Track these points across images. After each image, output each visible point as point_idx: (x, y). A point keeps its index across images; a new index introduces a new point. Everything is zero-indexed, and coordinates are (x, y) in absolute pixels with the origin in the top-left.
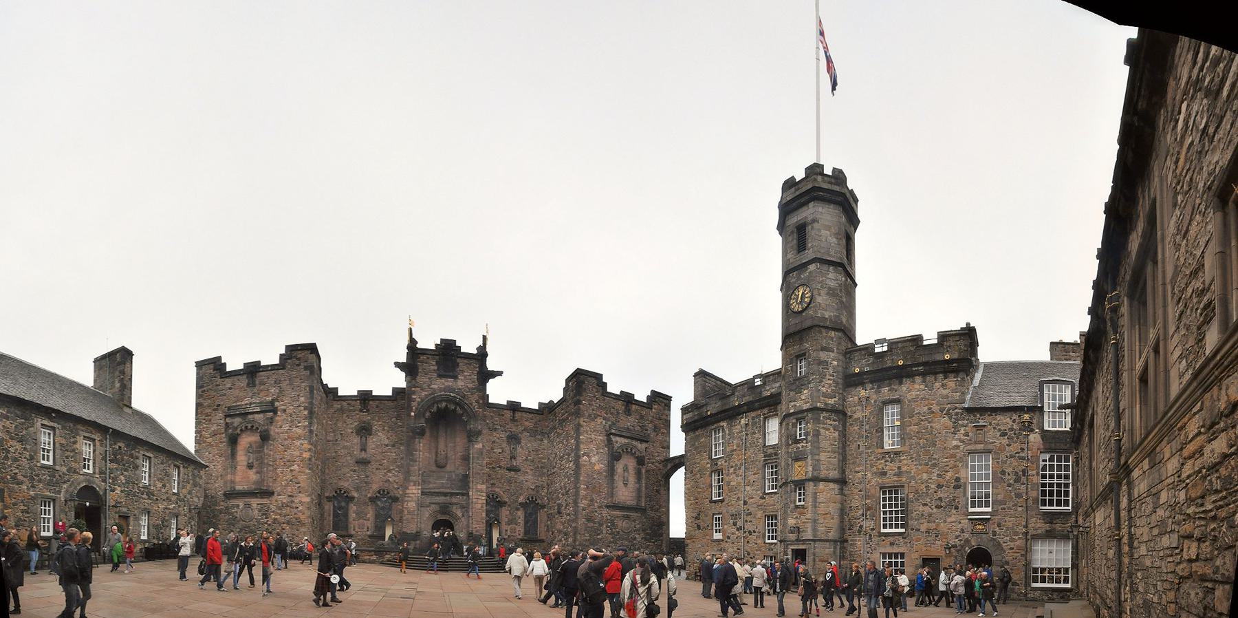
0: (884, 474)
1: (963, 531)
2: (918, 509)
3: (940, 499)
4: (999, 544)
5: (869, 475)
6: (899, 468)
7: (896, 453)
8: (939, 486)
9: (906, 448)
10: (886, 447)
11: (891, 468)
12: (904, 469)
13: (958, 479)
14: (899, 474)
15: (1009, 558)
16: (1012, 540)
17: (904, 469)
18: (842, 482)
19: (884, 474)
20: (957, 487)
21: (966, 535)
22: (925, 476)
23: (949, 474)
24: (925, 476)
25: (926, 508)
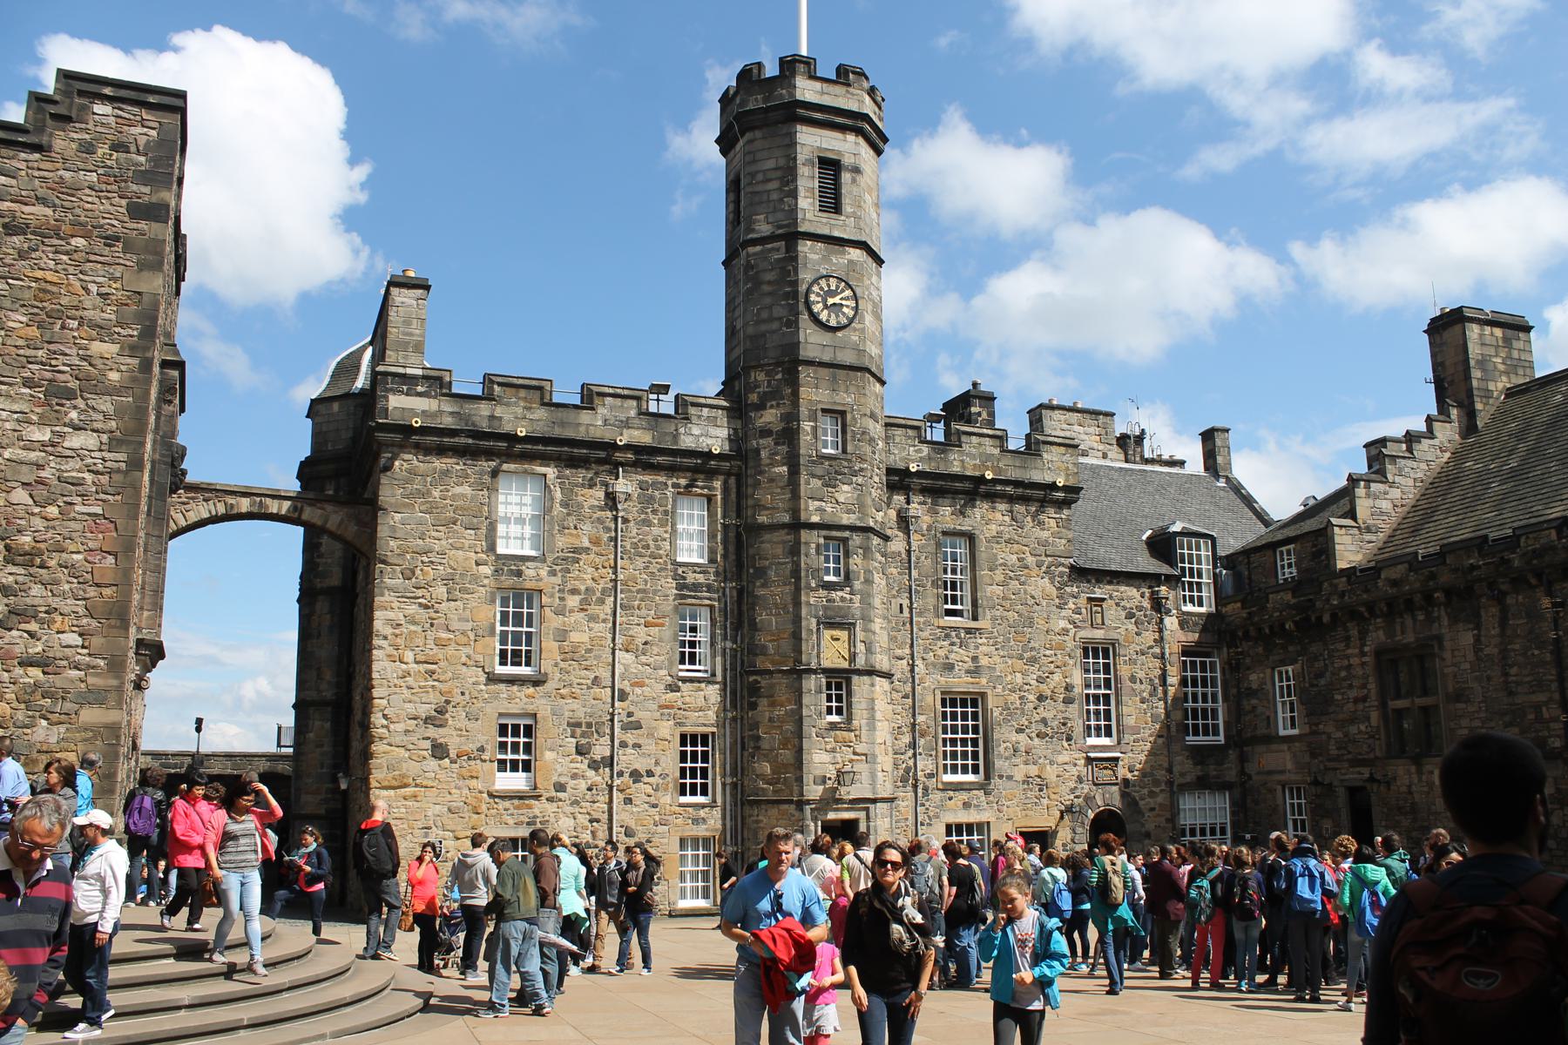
0: (949, 667)
1: (1080, 780)
2: (1005, 737)
3: (1044, 721)
4: (1136, 803)
6: (975, 659)
7: (969, 631)
8: (1041, 698)
11: (960, 655)
13: (1069, 688)
14: (975, 671)
15: (1150, 826)
16: (1152, 794)
17: (984, 661)
18: (888, 676)
19: (949, 667)
20: (1068, 701)
21: (1086, 788)
23: (1057, 677)
24: (1019, 678)
25: (1022, 737)
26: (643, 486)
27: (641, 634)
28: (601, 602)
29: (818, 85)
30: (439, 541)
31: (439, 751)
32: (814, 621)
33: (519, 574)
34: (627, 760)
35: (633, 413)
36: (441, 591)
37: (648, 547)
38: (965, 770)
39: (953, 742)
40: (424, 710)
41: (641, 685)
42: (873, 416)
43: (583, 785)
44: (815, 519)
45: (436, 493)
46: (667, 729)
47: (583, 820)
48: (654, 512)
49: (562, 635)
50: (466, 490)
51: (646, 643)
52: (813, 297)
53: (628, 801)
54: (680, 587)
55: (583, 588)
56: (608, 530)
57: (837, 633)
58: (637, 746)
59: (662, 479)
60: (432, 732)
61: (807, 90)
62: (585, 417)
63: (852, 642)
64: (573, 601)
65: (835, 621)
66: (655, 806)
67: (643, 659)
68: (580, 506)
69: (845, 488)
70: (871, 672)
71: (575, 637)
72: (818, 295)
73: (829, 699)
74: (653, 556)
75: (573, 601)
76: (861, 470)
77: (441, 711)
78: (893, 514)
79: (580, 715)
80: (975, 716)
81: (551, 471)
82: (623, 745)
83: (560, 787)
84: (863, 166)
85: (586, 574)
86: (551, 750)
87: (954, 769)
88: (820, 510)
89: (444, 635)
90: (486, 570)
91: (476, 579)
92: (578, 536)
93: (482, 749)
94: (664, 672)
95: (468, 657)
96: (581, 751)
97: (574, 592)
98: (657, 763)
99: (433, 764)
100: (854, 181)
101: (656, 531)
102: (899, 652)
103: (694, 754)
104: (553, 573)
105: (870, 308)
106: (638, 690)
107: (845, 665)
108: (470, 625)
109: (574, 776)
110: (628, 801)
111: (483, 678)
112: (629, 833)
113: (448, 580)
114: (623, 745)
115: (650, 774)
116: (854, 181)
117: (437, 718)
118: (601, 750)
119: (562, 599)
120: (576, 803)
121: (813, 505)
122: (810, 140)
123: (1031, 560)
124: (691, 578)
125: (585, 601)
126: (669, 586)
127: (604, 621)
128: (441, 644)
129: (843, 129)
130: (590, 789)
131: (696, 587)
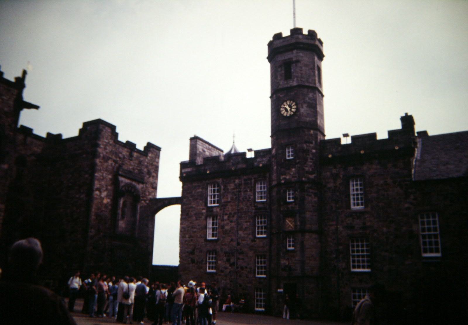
5: (340, 228)
9: (369, 209)
10: (352, 207)
12: (368, 224)
22: (385, 229)
24: (385, 229)
26: (245, 180)
27: (245, 225)
28: (233, 216)
29: (282, 41)
30: (194, 205)
31: (193, 261)
32: (281, 215)
33: (212, 211)
34: (240, 263)
35: (240, 160)
36: (194, 218)
37: (246, 198)
38: (364, 267)
39: (358, 256)
40: (190, 250)
41: (244, 240)
42: (306, 142)
43: (228, 271)
44: (283, 182)
45: (193, 192)
46: (251, 254)
47: (228, 281)
48: (249, 187)
49: (223, 227)
50: (200, 190)
51: (246, 228)
52: (282, 109)
53: (240, 276)
54: (256, 209)
55: (228, 213)
56: (235, 195)
57: (290, 219)
58: (243, 259)
59: (250, 176)
60: (191, 256)
61: (278, 43)
62: (227, 164)
63: (295, 221)
64: (226, 217)
65: (290, 214)
66: (247, 277)
67: (245, 232)
68: (228, 189)
69: (293, 169)
70: (303, 231)
71: (227, 227)
72: (283, 108)
73: (289, 242)
74: (248, 201)
75: (226, 217)
76: (299, 162)
77: (194, 250)
78: (328, 173)
79: (227, 250)
80: (367, 246)
81: (220, 181)
82: (239, 259)
83: (222, 271)
84: (300, 59)
85: (229, 208)
86: (220, 260)
87: (359, 267)
88: (285, 179)
89: (195, 230)
90: (204, 211)
91: (202, 214)
92: (227, 198)
93: (202, 261)
94: (250, 236)
95: (200, 235)
96: (228, 260)
97: (226, 214)
98: (248, 265)
99: (191, 265)
100: (296, 65)
101: (249, 193)
102: (331, 223)
103: (261, 262)
104: (221, 210)
105: (305, 106)
106: (243, 242)
107: (294, 229)
108: (200, 227)
109: (226, 268)
110: (240, 276)
111: (203, 241)
112: (241, 286)
113: (195, 214)
114: (239, 259)
115: (246, 268)
116: (296, 65)
117: (192, 253)
118: (232, 261)
119: (223, 217)
120: (226, 276)
121: (282, 177)
122: (281, 58)
123: (389, 181)
124: (259, 206)
125: (229, 217)
126: (252, 210)
127: (234, 222)
128: (194, 232)
129: (292, 50)
130: (230, 272)
131: (260, 209)
